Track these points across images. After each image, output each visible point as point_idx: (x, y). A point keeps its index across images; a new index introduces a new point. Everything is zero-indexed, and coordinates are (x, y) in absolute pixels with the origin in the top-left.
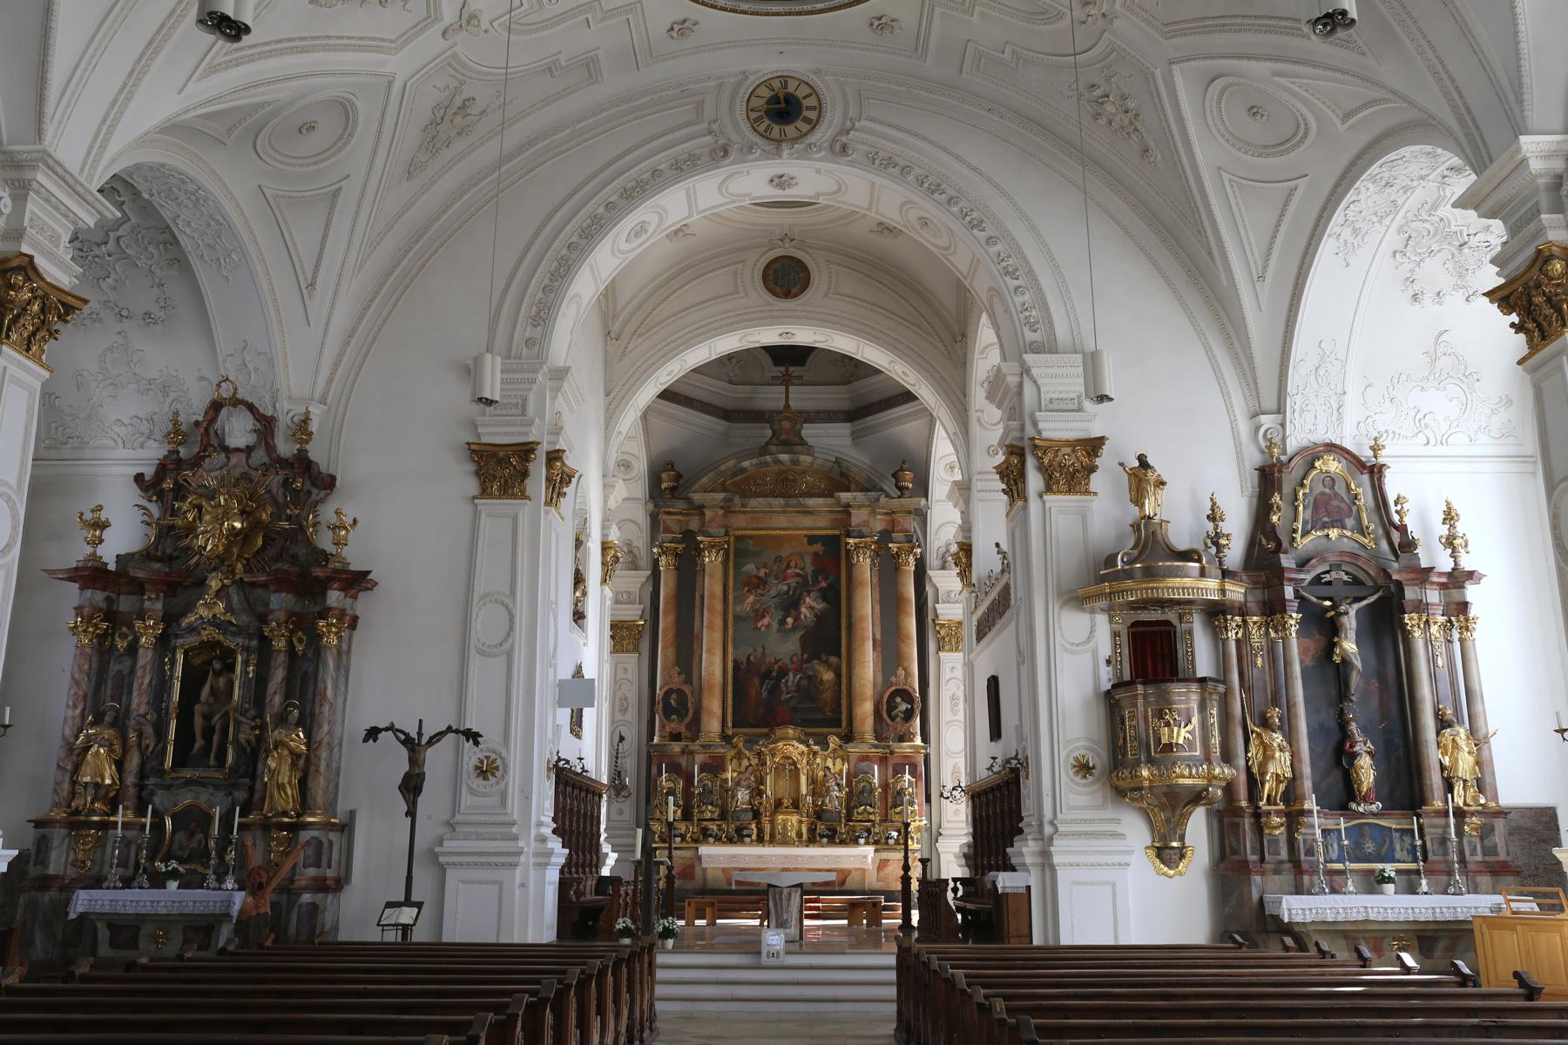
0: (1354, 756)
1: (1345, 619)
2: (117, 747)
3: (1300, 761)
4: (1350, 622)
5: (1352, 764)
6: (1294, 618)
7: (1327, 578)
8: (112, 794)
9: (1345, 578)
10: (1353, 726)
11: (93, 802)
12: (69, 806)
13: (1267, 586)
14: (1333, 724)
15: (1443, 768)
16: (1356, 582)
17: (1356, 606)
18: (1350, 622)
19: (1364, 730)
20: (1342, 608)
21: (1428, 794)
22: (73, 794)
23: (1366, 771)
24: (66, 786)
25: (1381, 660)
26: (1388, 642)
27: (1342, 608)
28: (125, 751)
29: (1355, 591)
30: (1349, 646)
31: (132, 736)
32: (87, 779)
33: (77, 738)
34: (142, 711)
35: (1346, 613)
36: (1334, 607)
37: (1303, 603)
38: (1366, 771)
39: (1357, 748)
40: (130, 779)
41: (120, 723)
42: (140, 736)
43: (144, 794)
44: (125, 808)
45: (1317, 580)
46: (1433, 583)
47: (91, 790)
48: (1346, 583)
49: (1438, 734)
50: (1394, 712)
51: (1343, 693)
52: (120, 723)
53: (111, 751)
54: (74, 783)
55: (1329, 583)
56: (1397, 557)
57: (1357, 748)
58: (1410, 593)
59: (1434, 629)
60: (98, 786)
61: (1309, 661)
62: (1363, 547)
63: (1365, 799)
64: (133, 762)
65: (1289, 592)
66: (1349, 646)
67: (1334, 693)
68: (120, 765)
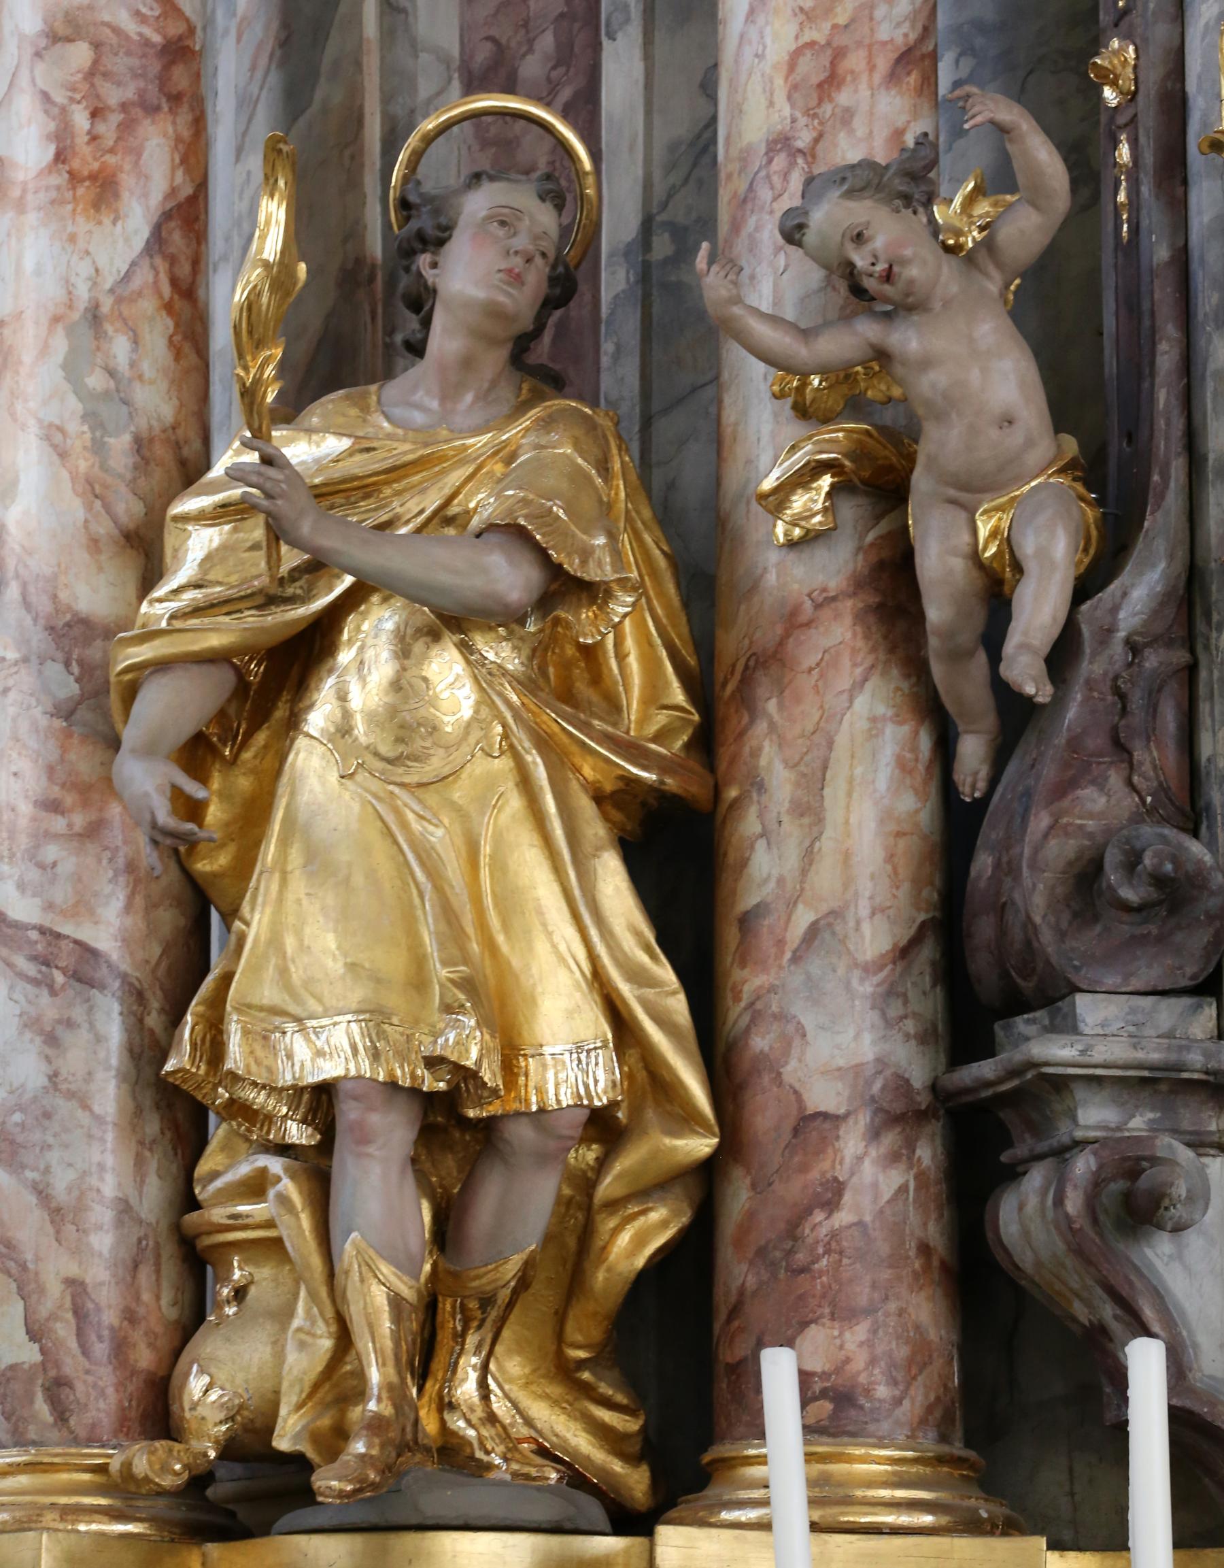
2: (633, 643)
8: (634, 1242)
11: (424, 1356)
12: (158, 1413)
22: (193, 1264)
24: (103, 1165)
28: (719, 685)
31: (772, 450)
32: (327, 1051)
33: (144, 551)
34: (876, 121)
40: (839, 1034)
41: (608, 337)
42: (880, 481)
43: (1026, 1216)
44: (833, 1411)
47: (381, 1190)
52: (608, 337)
53: (567, 681)
54: (180, 1119)
60: (455, 1127)
64: (839, 812)
68: (678, 854)
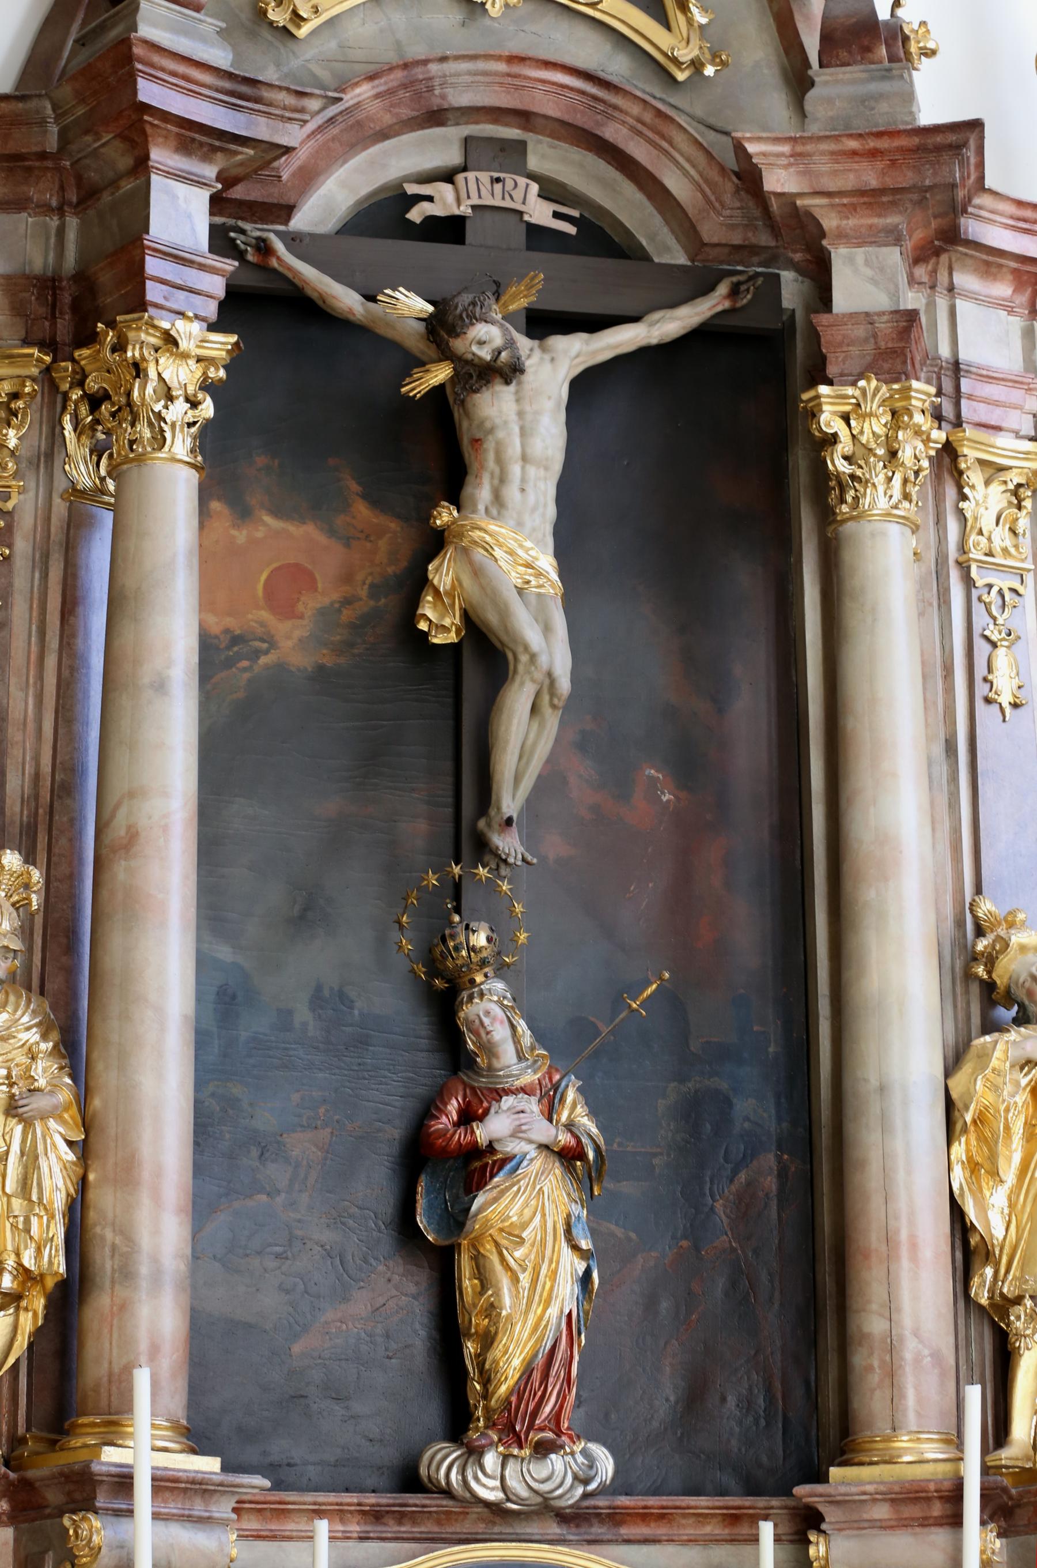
0: (478, 1166)
1: (495, 406)
3: (127, 1175)
4: (528, 425)
5: (456, 1219)
6: (182, 352)
7: (445, 200)
9: (540, 213)
10: (492, 1013)
13: (85, 195)
14: (389, 1001)
15: (967, 1247)
16: (597, 238)
17: (576, 352)
18: (528, 425)
19: (570, 1042)
20: (486, 337)
21: (872, 1402)
23: (538, 1259)
25: (702, 672)
26: (745, 579)
27: (486, 337)
29: (574, 283)
30: (512, 546)
35: (507, 371)
36: (442, 327)
37: (261, 306)
38: (538, 1259)
39: (494, 1127)
45: (386, 215)
46: (991, 261)
48: (536, 235)
49: (954, 1060)
50: (745, 930)
51: (468, 839)
55: (450, 230)
56: (798, 82)
57: (494, 1127)
58: (865, 281)
59: (986, 500)
61: (294, 642)
62: (659, 69)
63: (521, 1428)
65: (179, 211)
66: (512, 546)
67: (418, 826)
